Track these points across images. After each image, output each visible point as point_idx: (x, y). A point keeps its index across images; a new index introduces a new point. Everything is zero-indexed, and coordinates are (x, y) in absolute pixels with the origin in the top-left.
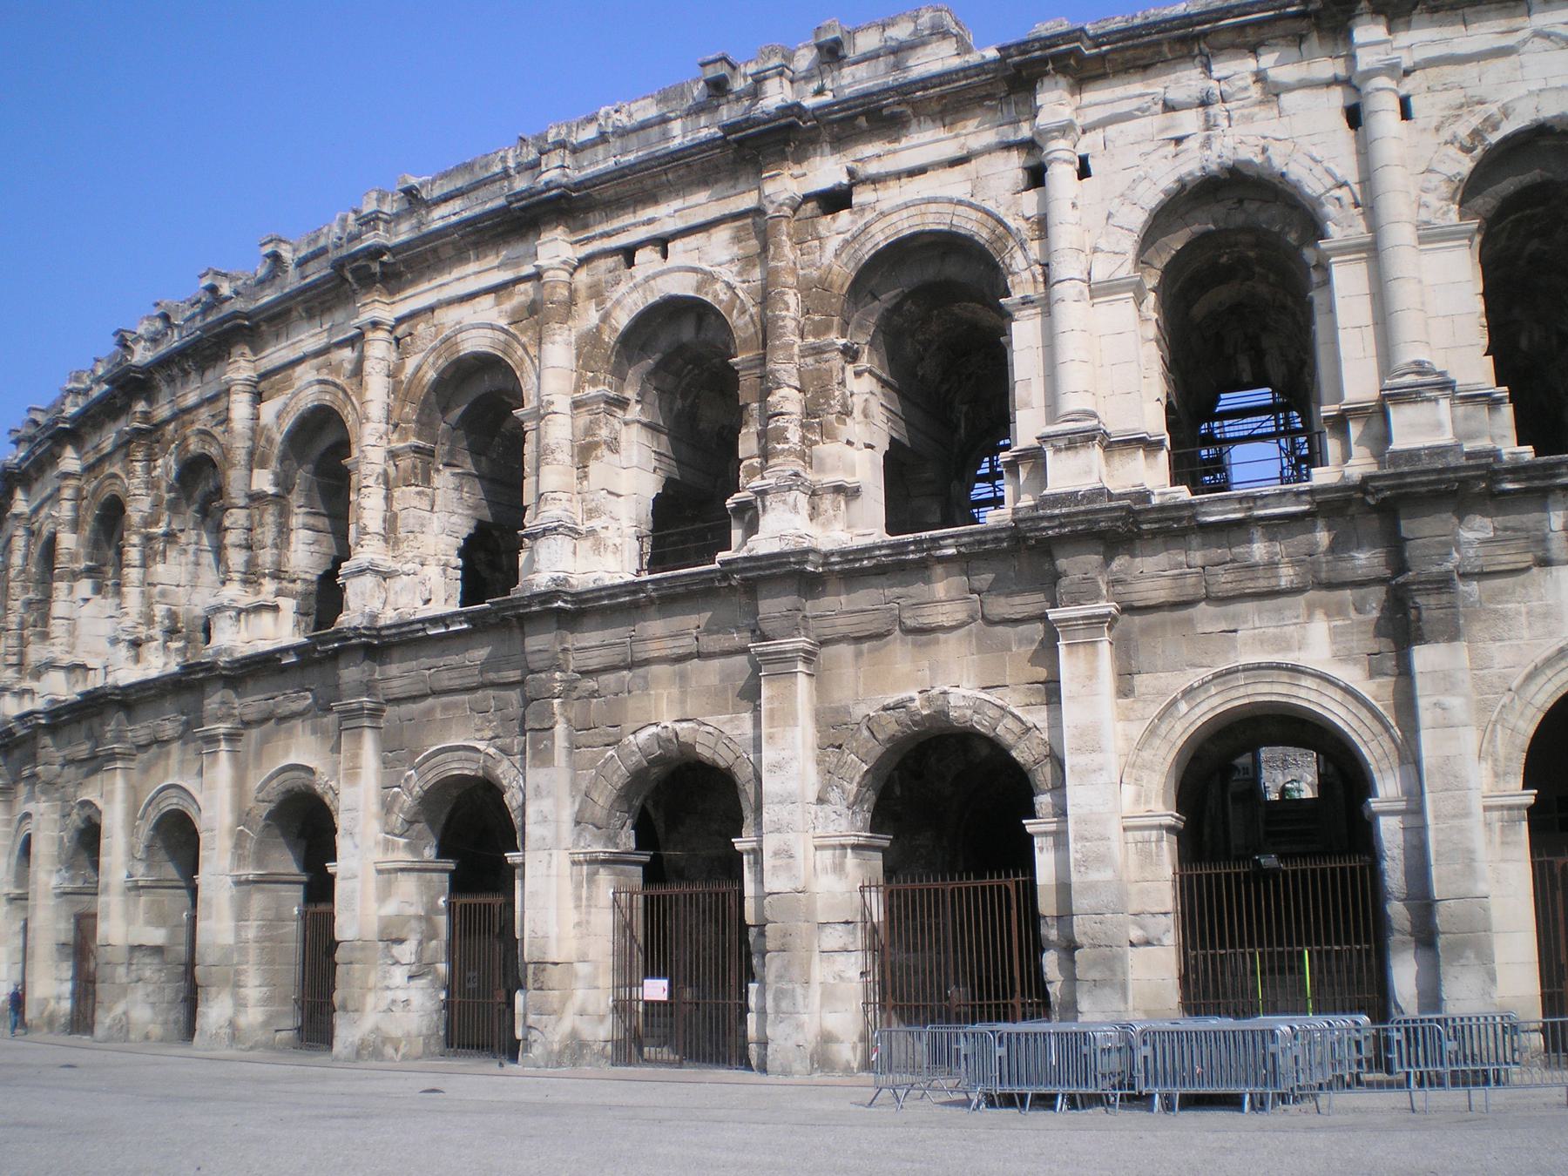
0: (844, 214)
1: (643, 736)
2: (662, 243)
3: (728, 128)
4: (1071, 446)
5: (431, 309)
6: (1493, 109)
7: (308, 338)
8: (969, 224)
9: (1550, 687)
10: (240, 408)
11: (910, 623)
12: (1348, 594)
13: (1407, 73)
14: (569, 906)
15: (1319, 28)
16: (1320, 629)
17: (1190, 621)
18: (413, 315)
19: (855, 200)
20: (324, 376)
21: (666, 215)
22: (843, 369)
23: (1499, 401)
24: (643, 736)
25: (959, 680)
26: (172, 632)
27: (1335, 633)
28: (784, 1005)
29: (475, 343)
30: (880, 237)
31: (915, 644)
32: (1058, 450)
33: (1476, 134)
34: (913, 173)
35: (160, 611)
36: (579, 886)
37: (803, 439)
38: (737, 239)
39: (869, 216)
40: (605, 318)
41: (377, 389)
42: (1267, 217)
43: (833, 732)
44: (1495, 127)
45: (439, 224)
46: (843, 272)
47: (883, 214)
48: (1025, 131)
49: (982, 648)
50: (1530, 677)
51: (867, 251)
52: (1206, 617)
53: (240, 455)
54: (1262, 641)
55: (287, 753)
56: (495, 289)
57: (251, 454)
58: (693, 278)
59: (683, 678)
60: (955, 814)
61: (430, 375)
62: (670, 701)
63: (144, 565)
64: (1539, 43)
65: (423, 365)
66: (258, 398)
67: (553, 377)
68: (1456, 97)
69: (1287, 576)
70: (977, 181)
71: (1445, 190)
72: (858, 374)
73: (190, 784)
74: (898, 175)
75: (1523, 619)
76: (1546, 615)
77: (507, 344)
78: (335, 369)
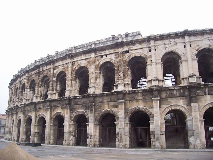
0: (128, 53)
1: (104, 110)
2: (106, 55)
3: (115, 43)
4: (155, 80)
5: (77, 61)
6: (200, 46)
7: (60, 63)
8: (142, 55)
9: (206, 108)
10: (52, 70)
11: (136, 99)
12: (184, 97)
13: (191, 42)
14: (93, 129)
15: (181, 37)
17: (167, 100)
18: (75, 61)
19: (129, 52)
20: (63, 67)
21: (107, 52)
23: (200, 78)
24: (104, 110)
25: (141, 105)
26: (41, 96)
27: (183, 102)
28: (121, 141)
30: (132, 56)
31: (137, 101)
32: (153, 81)
33: (198, 49)
34: (136, 49)
35: (40, 93)
36: (95, 127)
38: (115, 55)
39: (131, 54)
40: (99, 63)
41: (70, 69)
42: (175, 56)
43: (126, 110)
44: (200, 48)
45: (78, 51)
46: (128, 60)
47: (133, 54)
48: (149, 46)
49: (144, 102)
50: (204, 107)
51: (131, 58)
52: (169, 99)
53: (52, 76)
54: (175, 102)
55: (57, 110)
56: (86, 59)
57: (53, 76)
58: (110, 59)
59: (108, 104)
60: (140, 121)
61: (77, 68)
62: (107, 107)
63: (38, 88)
64: (205, 39)
65: (76, 67)
66: (54, 70)
67: (92, 70)
68: (196, 45)
69: (178, 95)
70: (143, 50)
71: (195, 55)
72: (129, 71)
73: (44, 114)
74: (134, 50)
75: (203, 101)
76: (206, 100)
77: (87, 65)
78: (65, 67)
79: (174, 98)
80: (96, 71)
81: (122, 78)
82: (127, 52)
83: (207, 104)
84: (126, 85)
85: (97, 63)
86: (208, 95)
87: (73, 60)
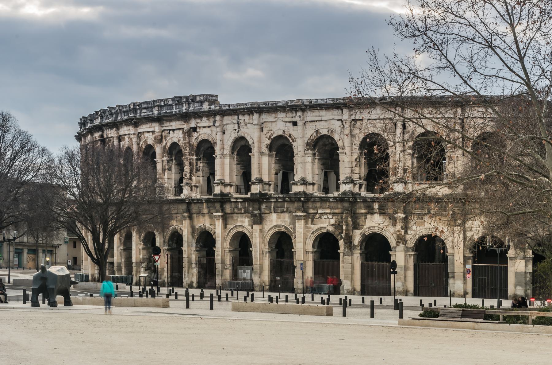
5: (144, 132)
6: (272, 132)
16: (247, 220)
17: (233, 217)
18: (141, 133)
22: (197, 163)
29: (150, 142)
30: (200, 139)
33: (270, 136)
37: (190, 176)
40: (166, 144)
50: (269, 231)
51: (198, 141)
61: (144, 147)
68: (268, 129)
69: (243, 211)
71: (266, 146)
79: (239, 215)
80: (163, 157)
81: (188, 175)
82: (195, 129)
83: (272, 227)
84: (193, 188)
85: (164, 143)
86: (275, 212)
87: (139, 131)
